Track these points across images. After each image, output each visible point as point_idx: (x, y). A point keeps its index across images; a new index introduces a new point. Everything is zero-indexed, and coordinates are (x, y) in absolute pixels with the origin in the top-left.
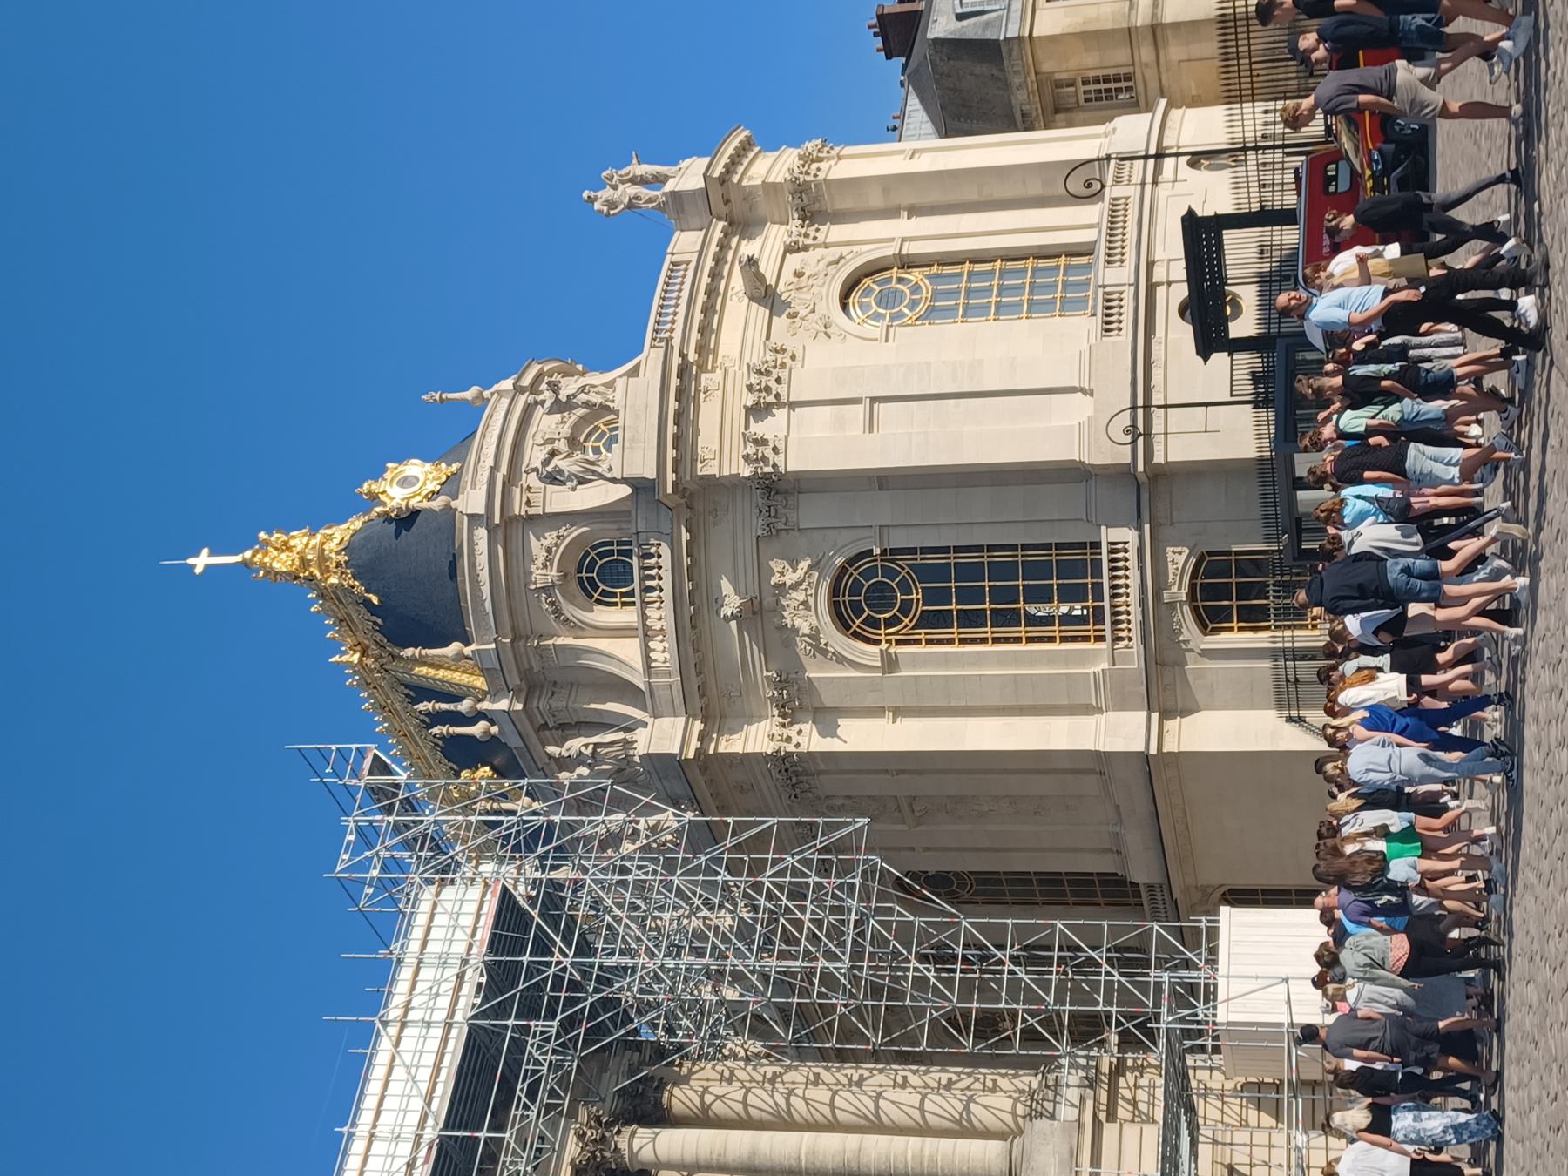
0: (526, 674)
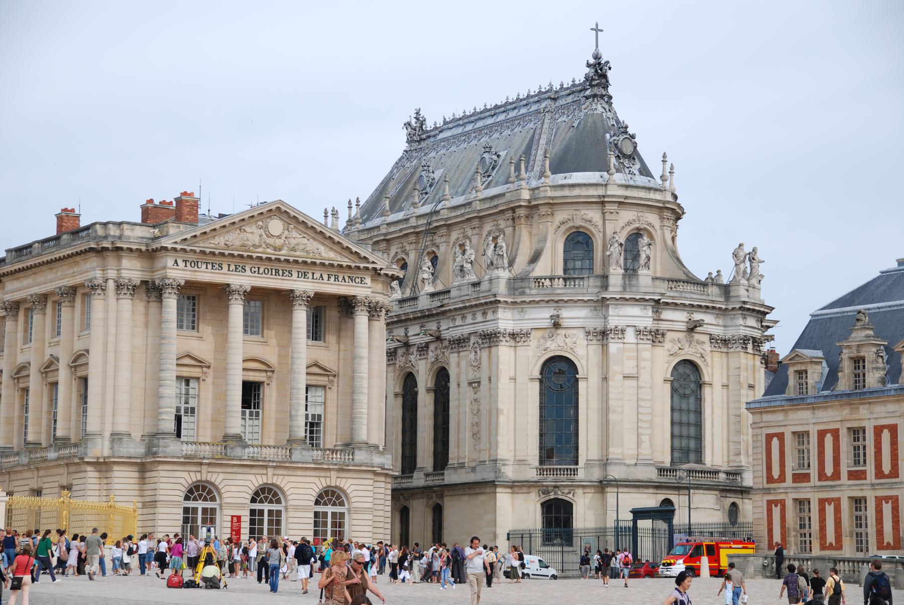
0: (536, 206)
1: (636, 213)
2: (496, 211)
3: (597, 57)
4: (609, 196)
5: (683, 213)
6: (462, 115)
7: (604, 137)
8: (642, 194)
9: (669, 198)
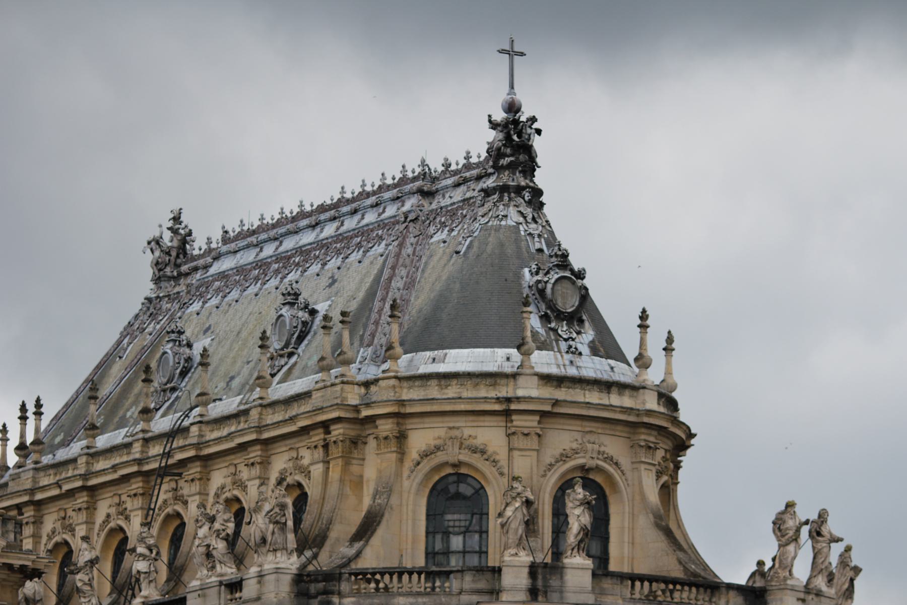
0: (371, 419)
1: (578, 436)
2: (293, 428)
3: (512, 108)
4: (518, 399)
5: (691, 436)
6: (257, 223)
7: (519, 277)
8: (594, 397)
9: (652, 403)
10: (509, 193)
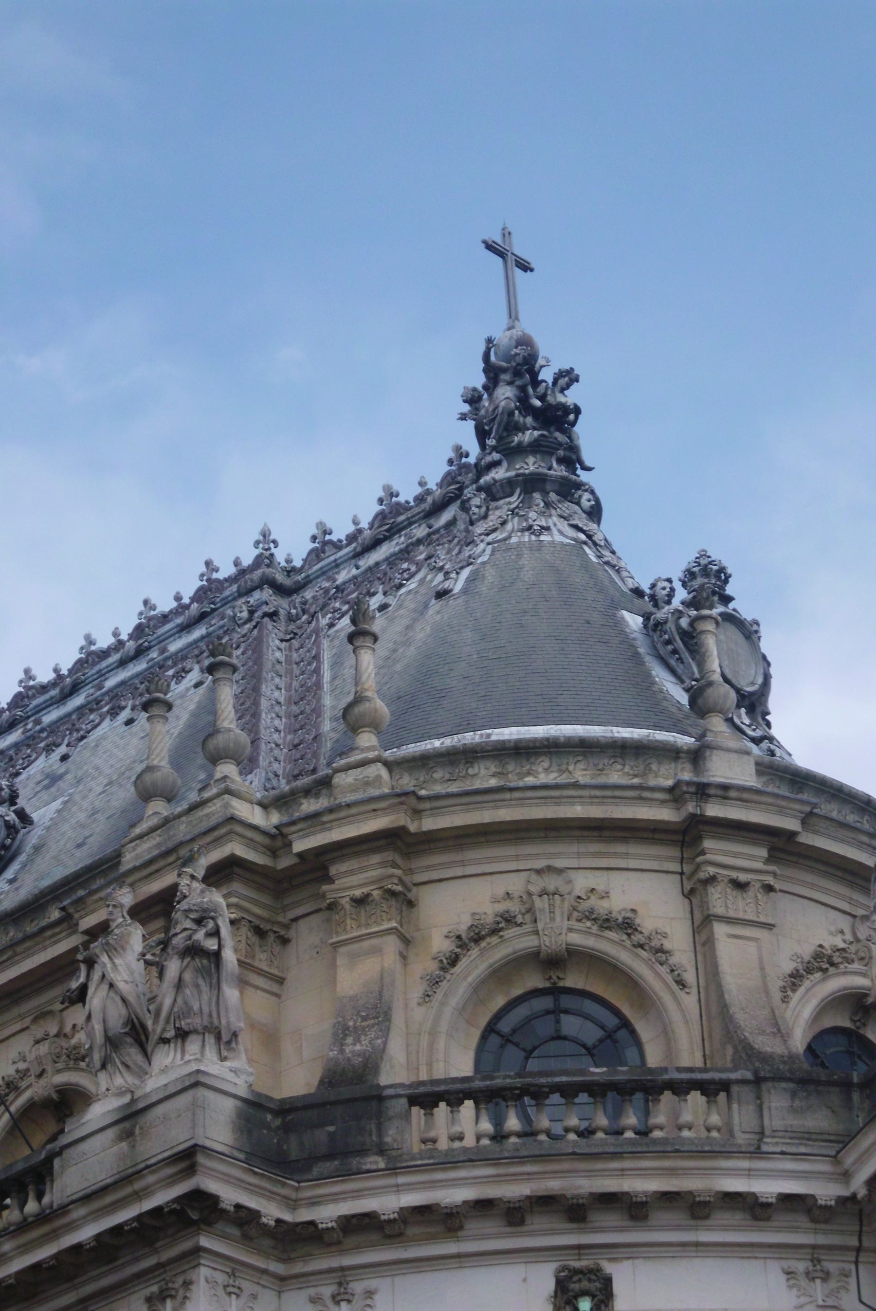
1: (844, 923)
10: (545, 493)
